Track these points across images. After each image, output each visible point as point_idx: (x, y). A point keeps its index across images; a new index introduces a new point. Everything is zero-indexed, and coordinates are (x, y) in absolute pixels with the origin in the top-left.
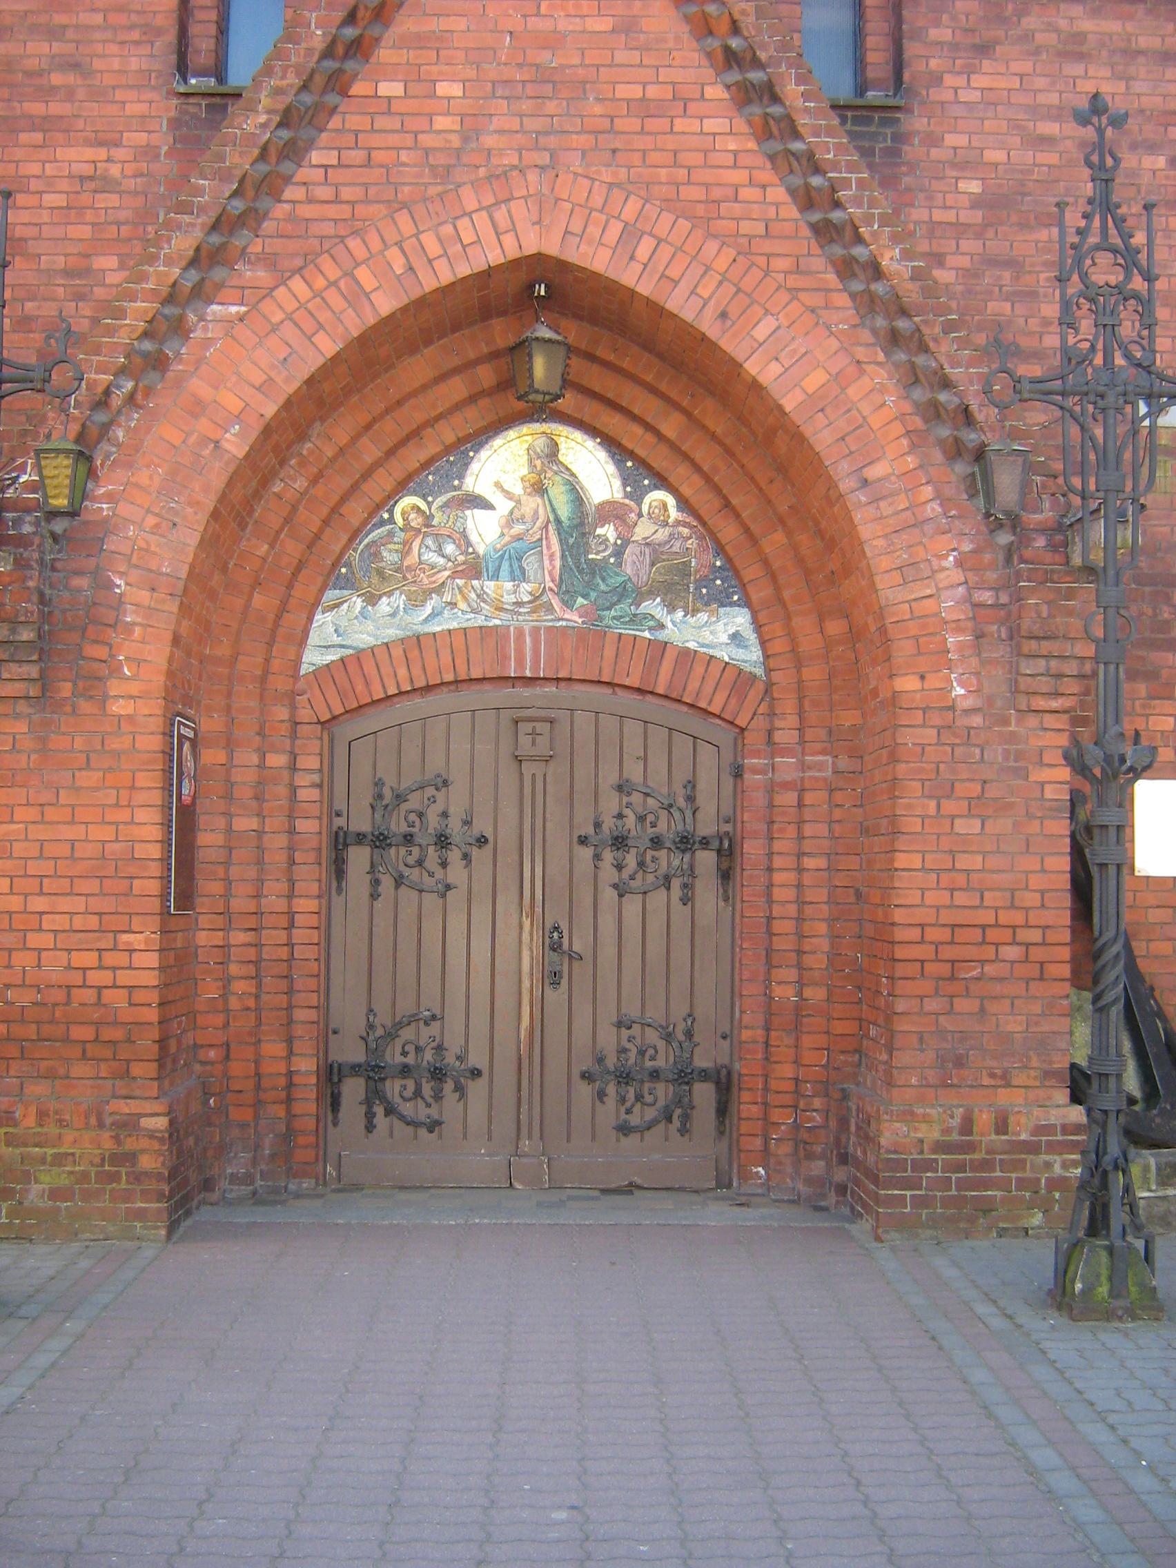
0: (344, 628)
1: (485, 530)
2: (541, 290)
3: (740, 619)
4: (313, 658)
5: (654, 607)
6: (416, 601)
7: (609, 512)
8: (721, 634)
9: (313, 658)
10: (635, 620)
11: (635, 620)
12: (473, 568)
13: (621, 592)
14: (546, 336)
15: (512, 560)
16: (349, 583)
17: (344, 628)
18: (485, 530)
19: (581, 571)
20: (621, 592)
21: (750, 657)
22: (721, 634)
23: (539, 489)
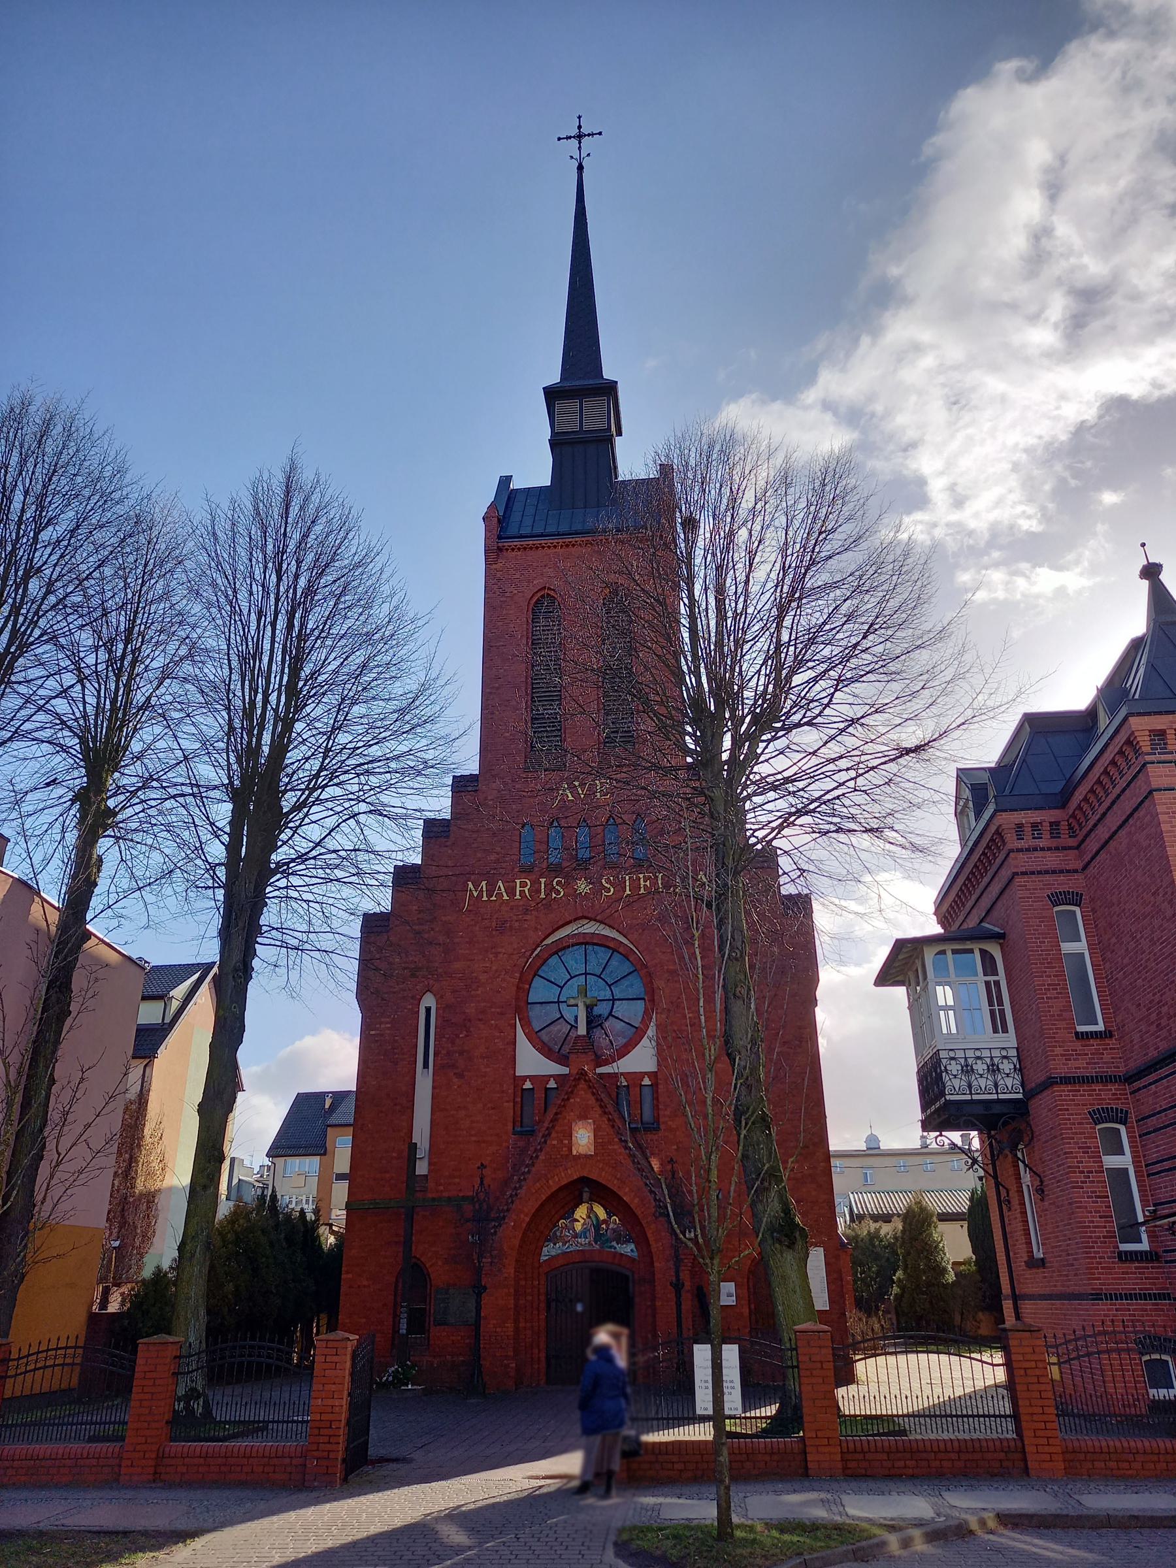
0: (550, 1251)
1: (578, 1227)
2: (584, 1181)
3: (632, 1246)
4: (543, 1258)
5: (614, 1243)
6: (564, 1244)
7: (604, 1221)
8: (628, 1249)
9: (543, 1258)
10: (611, 1247)
11: (611, 1247)
12: (576, 1236)
13: (607, 1240)
14: (586, 1188)
15: (584, 1233)
16: (549, 1240)
17: (550, 1251)
18: (578, 1227)
19: (598, 1236)
20: (607, 1240)
21: (635, 1254)
22: (628, 1249)
23: (589, 1217)
